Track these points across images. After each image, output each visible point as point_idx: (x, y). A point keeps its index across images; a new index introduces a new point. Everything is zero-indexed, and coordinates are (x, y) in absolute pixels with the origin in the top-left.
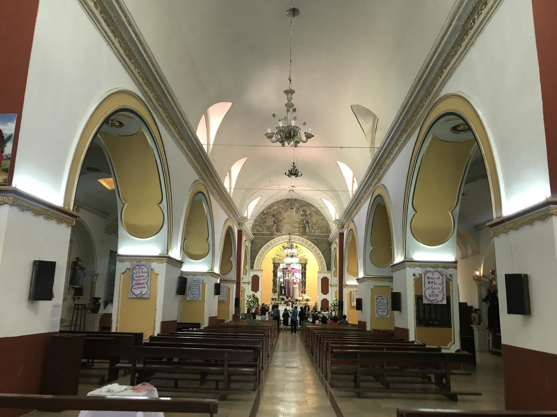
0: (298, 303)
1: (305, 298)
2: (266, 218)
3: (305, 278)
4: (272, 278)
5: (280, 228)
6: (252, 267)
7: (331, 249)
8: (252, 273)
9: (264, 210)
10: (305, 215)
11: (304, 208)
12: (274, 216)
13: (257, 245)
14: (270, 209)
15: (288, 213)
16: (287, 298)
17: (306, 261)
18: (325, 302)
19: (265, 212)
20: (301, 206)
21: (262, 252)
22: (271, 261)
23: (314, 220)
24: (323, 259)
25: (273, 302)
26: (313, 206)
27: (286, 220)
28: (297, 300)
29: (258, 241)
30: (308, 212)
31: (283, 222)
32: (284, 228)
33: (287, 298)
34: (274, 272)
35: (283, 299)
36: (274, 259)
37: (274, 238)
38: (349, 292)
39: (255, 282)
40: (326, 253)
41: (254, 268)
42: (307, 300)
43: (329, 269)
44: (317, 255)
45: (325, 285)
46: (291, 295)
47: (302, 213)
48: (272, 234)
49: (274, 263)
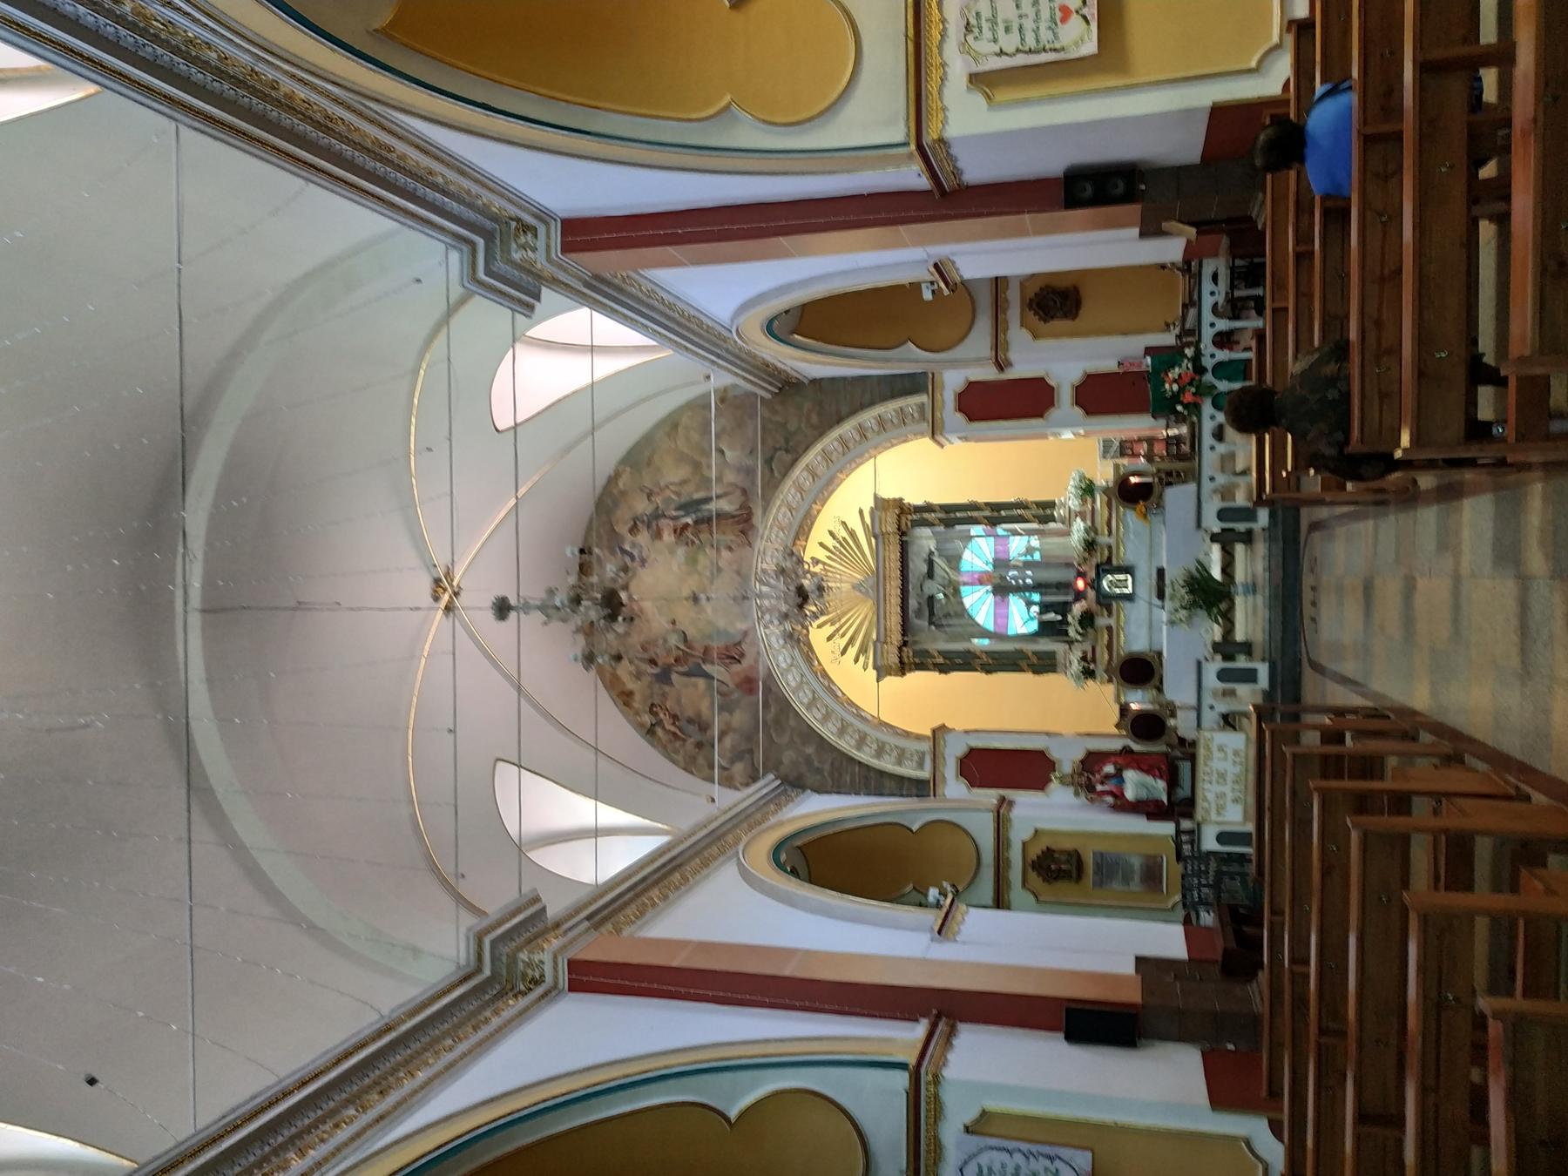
0: (1103, 539)
1: (1074, 504)
2: (675, 717)
3: (974, 507)
4: (978, 676)
5: (717, 644)
6: (921, 788)
7: (816, 382)
8: (954, 788)
9: (639, 726)
10: (652, 522)
11: (623, 529)
12: (664, 677)
13: (808, 760)
14: (630, 694)
15: (647, 605)
16: (1079, 596)
17: (881, 504)
18: (1098, 395)
19: (647, 719)
20: (614, 543)
21: (842, 732)
22: (891, 682)
23: (673, 474)
24: (868, 417)
25: (1100, 670)
26: (613, 480)
27: (687, 617)
28: (1090, 545)
29: (788, 756)
30: (642, 506)
31: (692, 633)
32: (721, 623)
33: (1079, 596)
34: (943, 669)
35: (1087, 620)
36: (882, 672)
37: (770, 675)
38: (979, 100)
39: (1005, 767)
40: (830, 404)
41: (925, 774)
42: (1088, 489)
43: (912, 384)
44: (850, 456)
45: (1006, 403)
46: (1067, 575)
47: (643, 537)
48: (748, 684)
49: (903, 668)
